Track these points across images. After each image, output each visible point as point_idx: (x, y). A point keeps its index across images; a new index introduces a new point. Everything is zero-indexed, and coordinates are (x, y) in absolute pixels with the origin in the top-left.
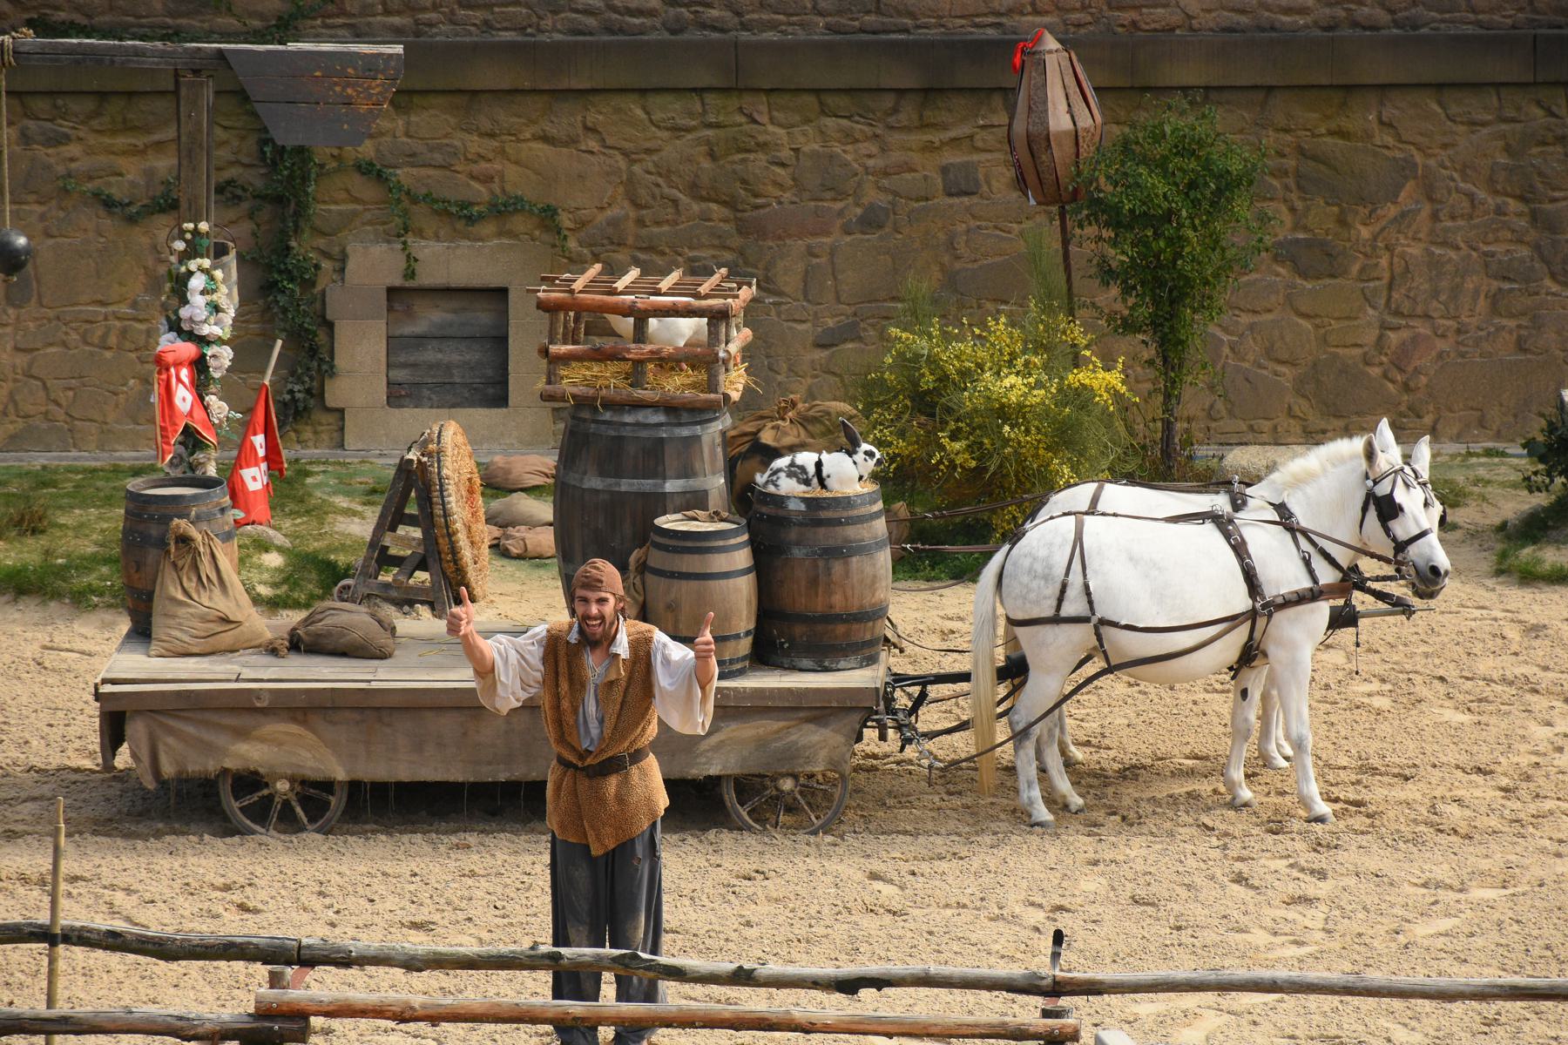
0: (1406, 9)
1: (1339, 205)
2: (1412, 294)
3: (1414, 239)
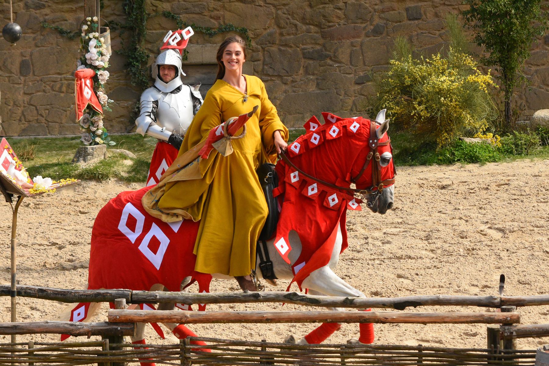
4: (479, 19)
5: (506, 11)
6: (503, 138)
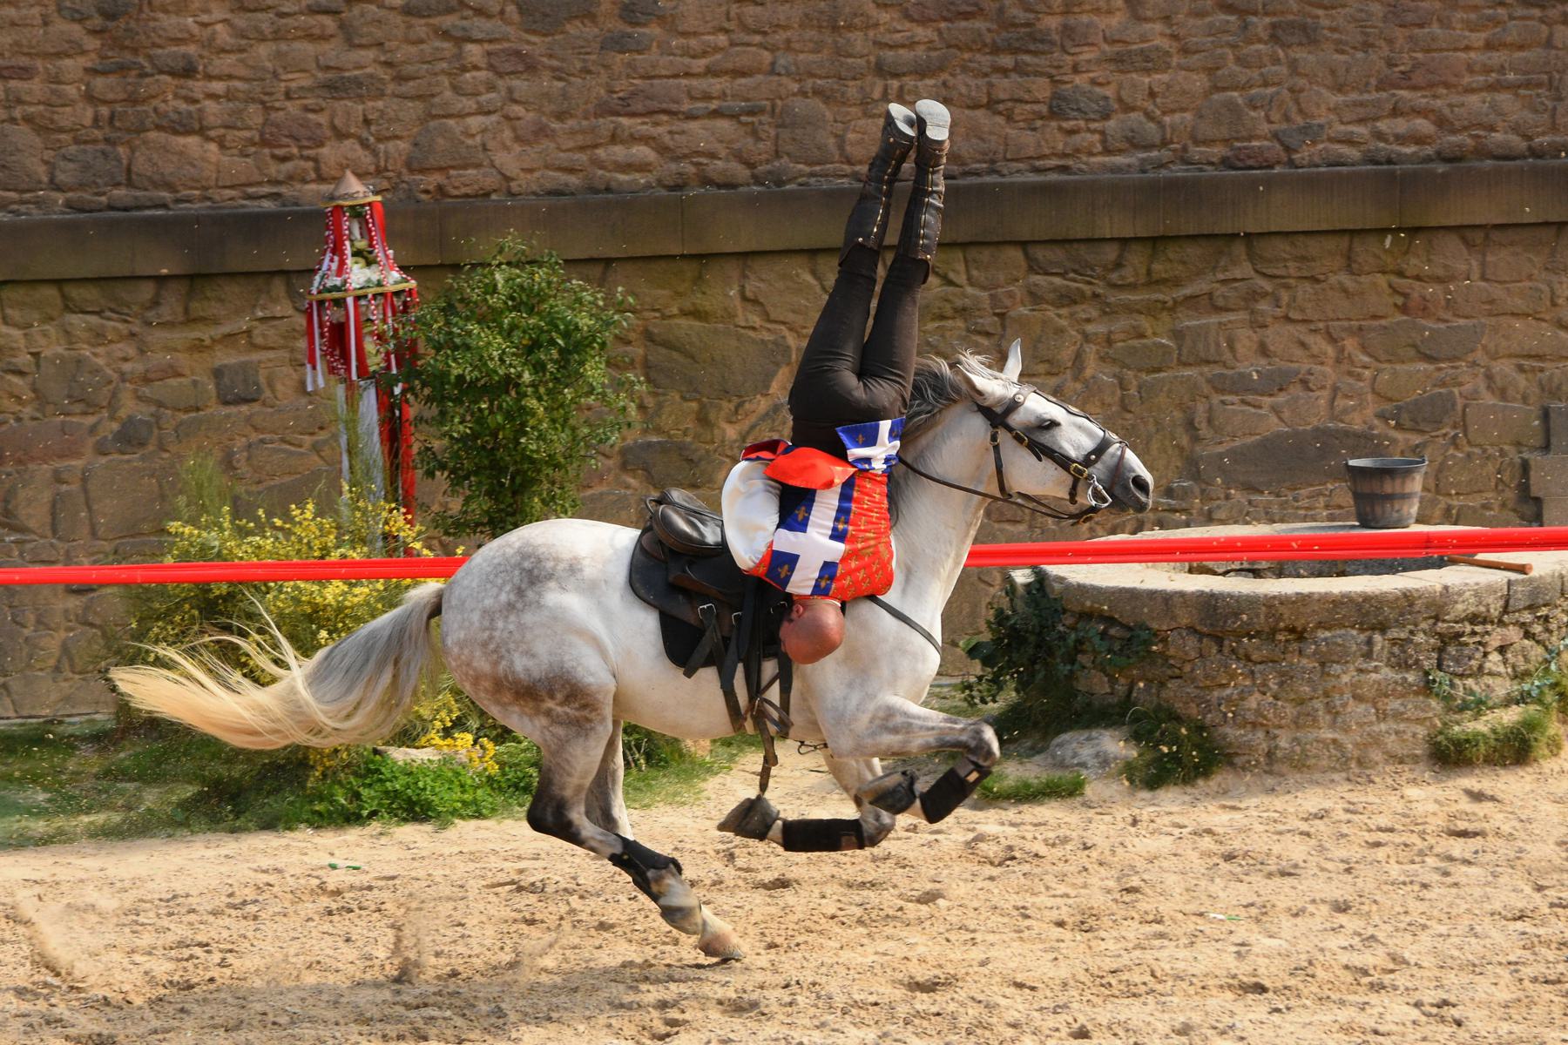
0: (768, 161)
1: (699, 401)
4: (429, 399)
5: (508, 376)
6: (502, 749)
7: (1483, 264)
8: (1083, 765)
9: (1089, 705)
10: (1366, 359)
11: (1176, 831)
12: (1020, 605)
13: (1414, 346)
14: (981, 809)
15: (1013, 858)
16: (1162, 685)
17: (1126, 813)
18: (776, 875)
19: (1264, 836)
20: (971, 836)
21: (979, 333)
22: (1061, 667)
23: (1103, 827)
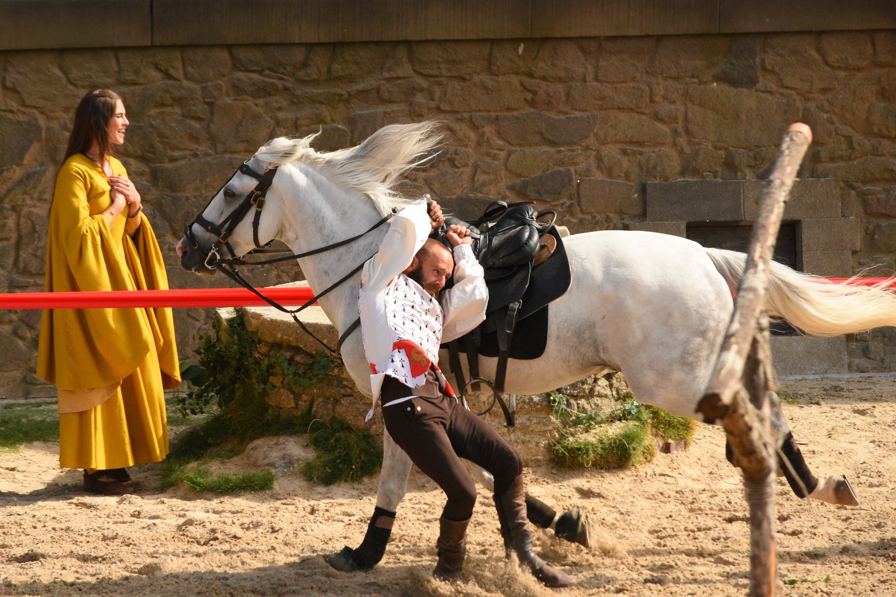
2: (39, 253)
3: (40, 199)
7: (597, 68)
8: (272, 465)
9: (278, 417)
10: (501, 143)
11: (346, 519)
12: (224, 336)
13: (541, 133)
14: (189, 500)
15: (216, 539)
16: (337, 401)
17: (306, 503)
18: (26, 551)
19: (417, 523)
20: (182, 521)
21: (193, 118)
22: (256, 386)
23: (287, 515)
